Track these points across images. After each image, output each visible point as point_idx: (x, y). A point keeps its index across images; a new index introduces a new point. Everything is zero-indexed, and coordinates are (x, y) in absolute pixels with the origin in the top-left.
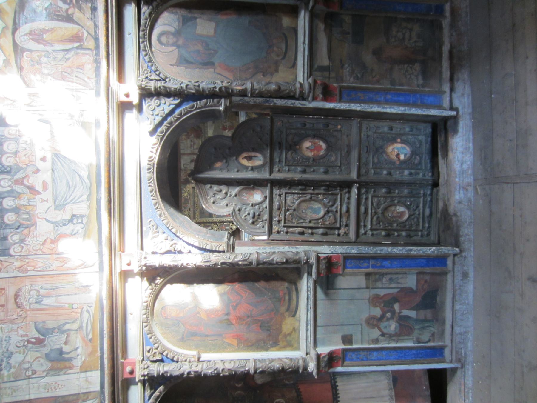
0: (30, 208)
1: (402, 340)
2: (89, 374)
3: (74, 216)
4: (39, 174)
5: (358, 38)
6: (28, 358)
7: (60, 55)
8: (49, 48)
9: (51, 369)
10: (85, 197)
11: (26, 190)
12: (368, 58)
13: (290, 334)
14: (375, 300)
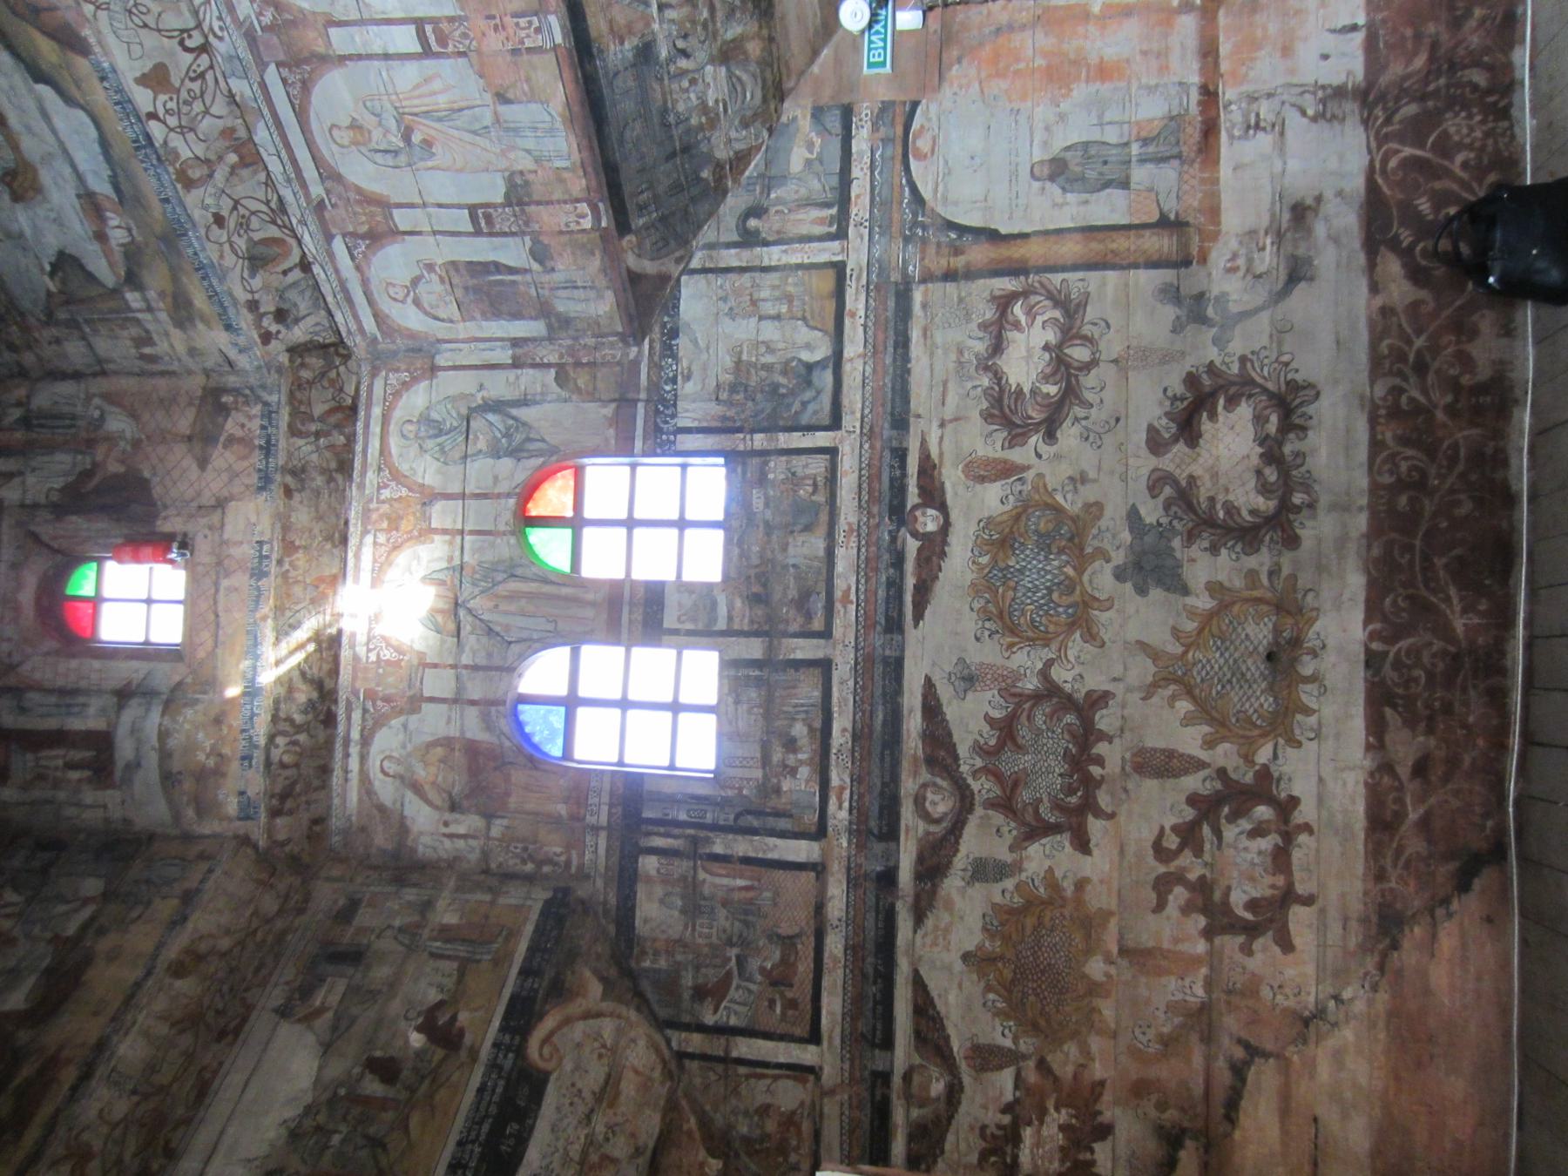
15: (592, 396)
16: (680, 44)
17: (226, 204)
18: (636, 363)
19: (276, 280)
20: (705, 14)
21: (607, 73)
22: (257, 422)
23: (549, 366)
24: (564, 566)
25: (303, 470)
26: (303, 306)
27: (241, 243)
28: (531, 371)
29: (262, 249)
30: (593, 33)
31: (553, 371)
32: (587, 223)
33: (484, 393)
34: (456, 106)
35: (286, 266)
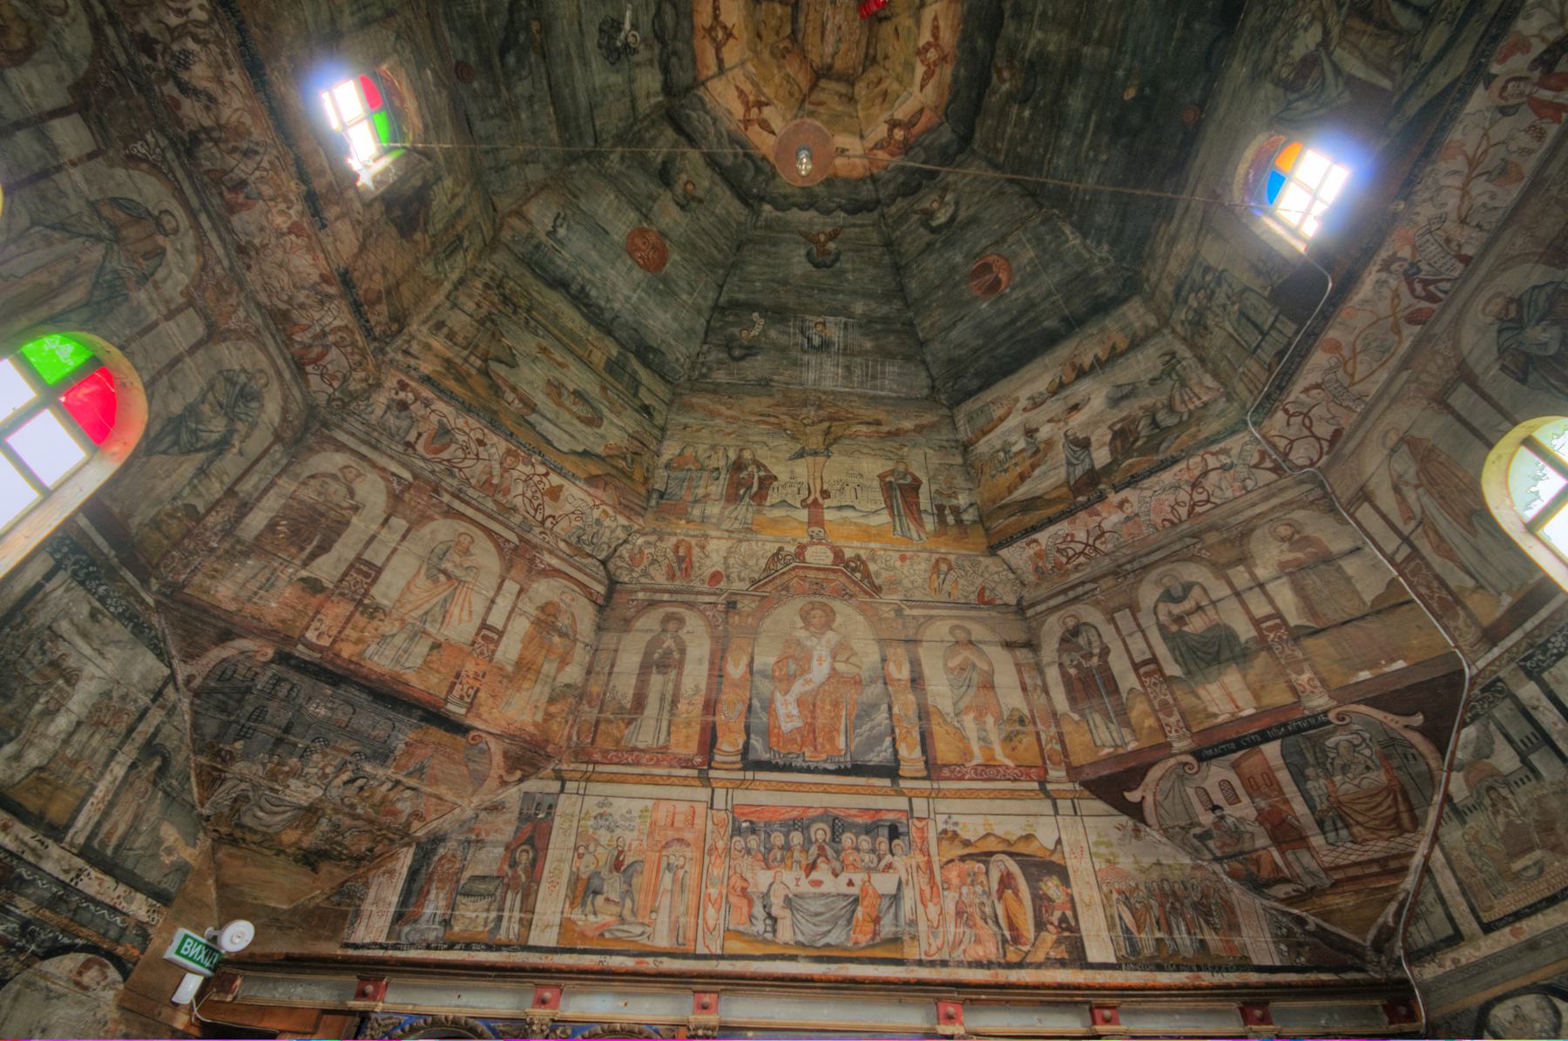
0: (788, 862)
2: (556, 930)
3: (775, 920)
4: (831, 876)
6: (600, 850)
7: (988, 910)
8: (995, 896)
9: (578, 878)
10: (800, 938)
11: (811, 859)
15: (156, 524)
16: (360, 782)
17: (484, 455)
18: (145, 582)
19: (423, 427)
20: (359, 811)
21: (401, 721)
22: (373, 323)
23: (208, 512)
24: (30, 349)
25: (322, 303)
26: (391, 420)
27: (461, 438)
28: (217, 496)
29: (447, 439)
31: (202, 510)
32: (311, 635)
33: (235, 450)
35: (422, 440)
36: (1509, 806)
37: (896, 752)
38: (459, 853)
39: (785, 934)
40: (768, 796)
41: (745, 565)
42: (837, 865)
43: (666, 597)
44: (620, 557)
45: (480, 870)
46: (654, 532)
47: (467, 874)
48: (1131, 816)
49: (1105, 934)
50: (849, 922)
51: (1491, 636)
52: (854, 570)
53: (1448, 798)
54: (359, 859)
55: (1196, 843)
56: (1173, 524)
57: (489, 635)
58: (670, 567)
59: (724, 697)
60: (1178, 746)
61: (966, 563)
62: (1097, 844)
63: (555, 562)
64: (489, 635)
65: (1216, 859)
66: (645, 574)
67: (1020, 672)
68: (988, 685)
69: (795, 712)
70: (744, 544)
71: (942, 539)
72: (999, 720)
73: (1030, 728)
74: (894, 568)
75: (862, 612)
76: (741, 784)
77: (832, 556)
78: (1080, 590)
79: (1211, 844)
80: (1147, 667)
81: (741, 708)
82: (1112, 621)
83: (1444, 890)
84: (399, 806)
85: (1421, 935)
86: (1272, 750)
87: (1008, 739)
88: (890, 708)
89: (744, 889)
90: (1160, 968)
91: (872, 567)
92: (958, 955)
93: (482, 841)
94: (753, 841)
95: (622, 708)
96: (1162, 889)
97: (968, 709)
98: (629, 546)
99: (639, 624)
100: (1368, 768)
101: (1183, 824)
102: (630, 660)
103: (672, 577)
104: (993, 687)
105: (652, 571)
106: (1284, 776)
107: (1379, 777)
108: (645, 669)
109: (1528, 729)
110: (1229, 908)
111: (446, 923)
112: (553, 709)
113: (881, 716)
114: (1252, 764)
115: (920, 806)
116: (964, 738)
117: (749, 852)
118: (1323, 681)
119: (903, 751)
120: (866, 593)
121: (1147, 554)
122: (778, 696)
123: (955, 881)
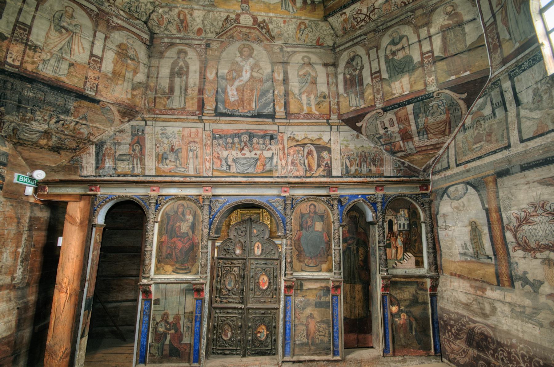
0: (234, 148)
1: (152, 336)
2: (154, 170)
3: (230, 166)
5: (318, 305)
6: (165, 145)
7: (302, 162)
10: (238, 171)
11: (242, 147)
12: (308, 311)
13: (163, 269)
14: (177, 318)
16: (61, 122)
20: (66, 133)
21: (68, 98)
30: (83, 101)
34: (72, 50)
36: (481, 127)
37: (274, 109)
38: (112, 147)
39: (233, 170)
40: (225, 126)
41: (212, 25)
42: (251, 149)
43: (178, 41)
44: (153, 19)
45: (122, 153)
46: (166, 6)
47: (117, 154)
48: (357, 131)
49: (339, 168)
50: (255, 166)
51: (504, 61)
52: (262, 28)
53: (464, 124)
54: (75, 150)
55: (377, 140)
56: (406, 5)
57: (95, 60)
58: (177, 25)
59: (206, 87)
60: (378, 106)
61: (313, 25)
62: (343, 140)
63: (119, 22)
64: (95, 60)
65: (382, 145)
66: (166, 29)
67: (328, 77)
68: (314, 82)
69: (235, 93)
70: (211, 13)
71: (303, 12)
72: (316, 97)
73: (328, 100)
74: (281, 27)
75: (266, 49)
76: (215, 122)
77: (252, 20)
78: (359, 39)
79: (381, 140)
80: (376, 75)
81: (214, 92)
82: (368, 54)
83: (450, 154)
84: (82, 131)
85: (438, 167)
86: (410, 107)
87: (318, 104)
88: (274, 92)
89: (218, 157)
90: (355, 177)
91: (271, 27)
92: (291, 174)
93: (120, 143)
94: (221, 141)
95: (164, 92)
96: (361, 155)
97: (305, 92)
98: (156, 14)
99: (167, 54)
100: (441, 114)
101: (374, 133)
102: (165, 71)
103: (179, 31)
104: (316, 83)
105: (169, 27)
106: (411, 117)
107: (444, 117)
108: (172, 75)
109: (500, 99)
110: (382, 160)
111: (115, 169)
112: (135, 93)
113: (270, 95)
114: (402, 112)
115: (282, 128)
116: (302, 103)
117: (219, 145)
118: (437, 80)
119: (277, 109)
120: (268, 40)
121: (391, 21)
122: (228, 87)
123: (292, 153)
